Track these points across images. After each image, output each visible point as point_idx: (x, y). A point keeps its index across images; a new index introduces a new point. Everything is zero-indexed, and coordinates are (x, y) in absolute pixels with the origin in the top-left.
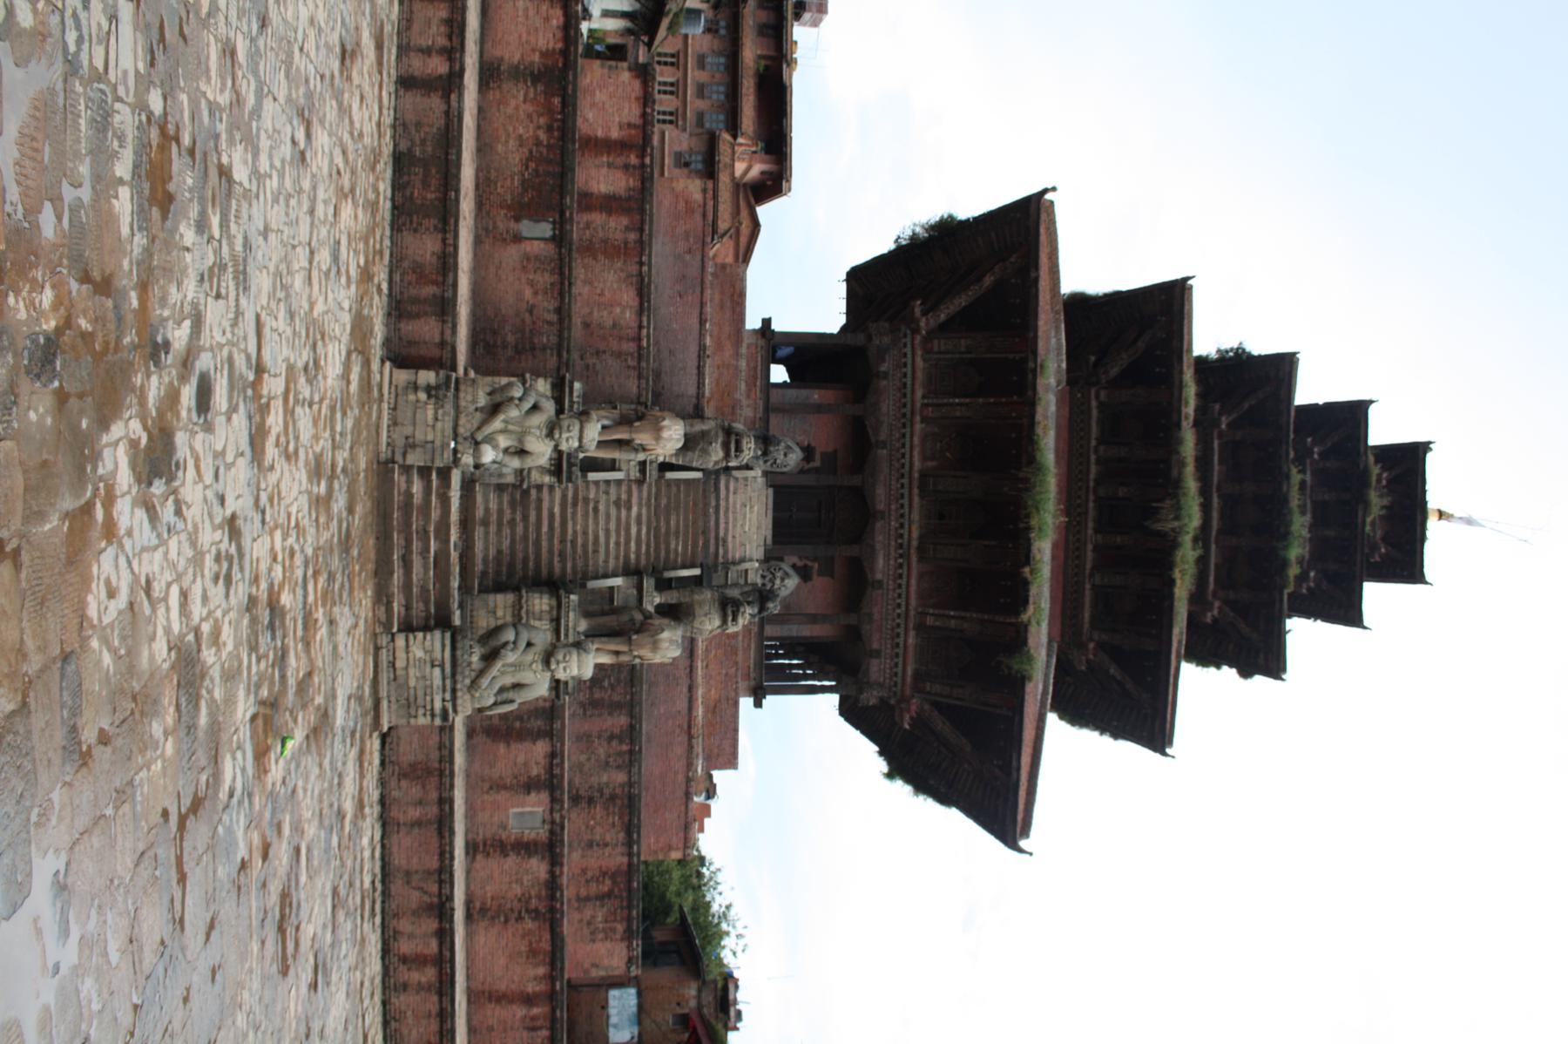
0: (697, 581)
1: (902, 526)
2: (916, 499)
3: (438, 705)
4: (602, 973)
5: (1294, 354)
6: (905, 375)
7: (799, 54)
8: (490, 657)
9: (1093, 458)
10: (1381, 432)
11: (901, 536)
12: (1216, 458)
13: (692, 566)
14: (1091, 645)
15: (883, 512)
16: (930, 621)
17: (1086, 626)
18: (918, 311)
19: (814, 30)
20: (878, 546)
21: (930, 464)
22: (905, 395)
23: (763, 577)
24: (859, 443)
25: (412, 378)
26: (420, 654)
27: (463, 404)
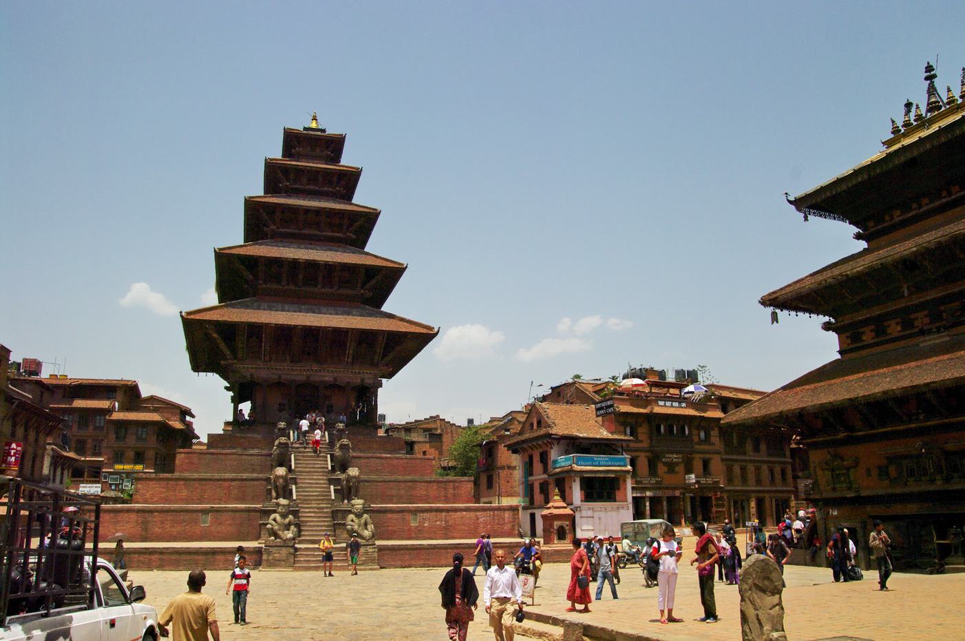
4: (473, 491)
5: (245, 199)
6: (252, 367)
7: (59, 373)
9: (286, 287)
10: (276, 152)
11: (316, 370)
12: (288, 230)
13: (326, 457)
14: (362, 291)
15: (307, 377)
16: (350, 360)
17: (355, 292)
18: (225, 363)
19: (43, 364)
21: (288, 358)
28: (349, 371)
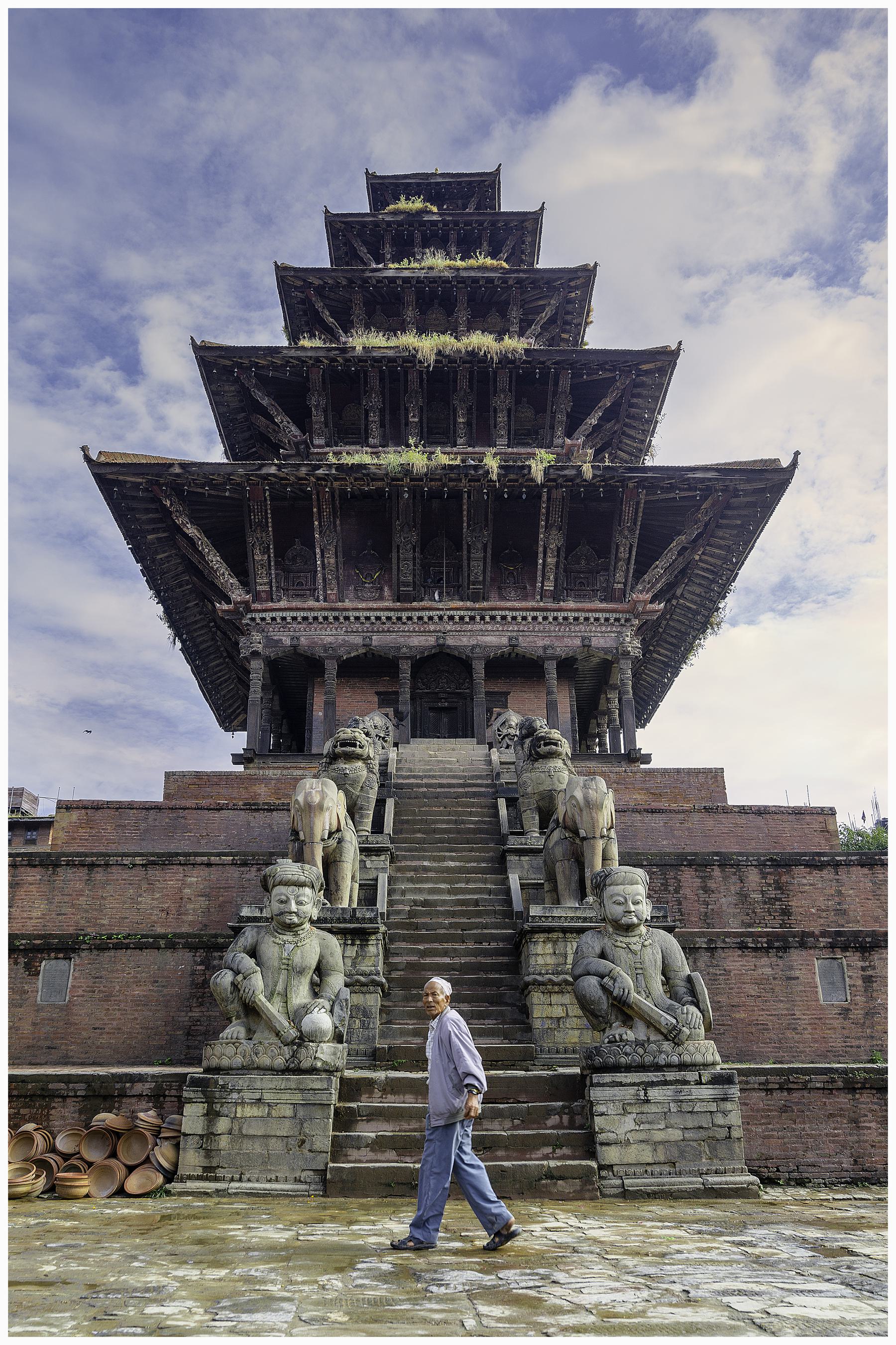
0: (512, 803)
1: (451, 618)
2: (422, 604)
3: (706, 1092)
6: (294, 619)
8: (624, 1010)
11: (462, 618)
13: (495, 807)
14: (568, 441)
16: (549, 586)
18: (225, 607)
20: (475, 642)
21: (387, 592)
22: (316, 618)
23: (508, 747)
24: (369, 669)
25: (192, 1142)
26: (629, 1123)
27: (238, 1061)
28: (551, 616)
